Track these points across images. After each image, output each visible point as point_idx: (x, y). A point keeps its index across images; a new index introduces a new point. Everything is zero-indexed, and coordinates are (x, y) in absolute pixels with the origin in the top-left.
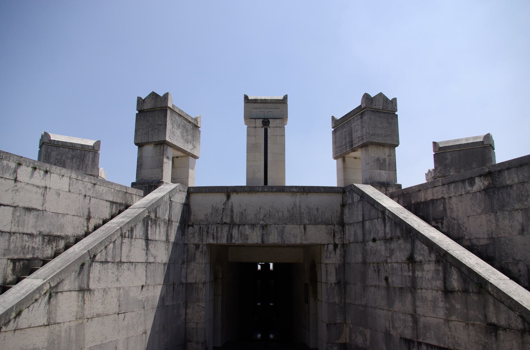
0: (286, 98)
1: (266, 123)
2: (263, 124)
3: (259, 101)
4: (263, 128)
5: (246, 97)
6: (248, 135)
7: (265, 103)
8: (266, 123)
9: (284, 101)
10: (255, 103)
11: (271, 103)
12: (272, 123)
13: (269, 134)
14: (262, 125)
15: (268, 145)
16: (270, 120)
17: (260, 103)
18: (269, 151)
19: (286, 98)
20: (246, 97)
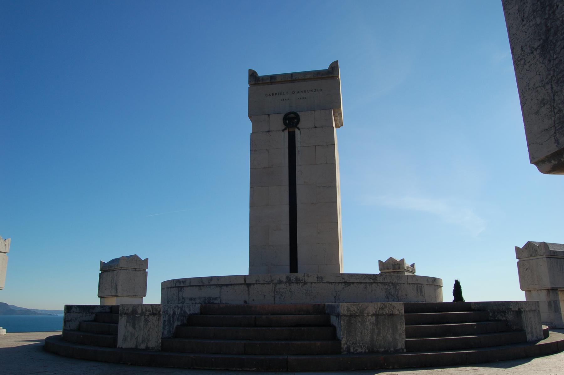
0: (334, 67)
1: (291, 121)
2: (285, 123)
3: (279, 80)
4: (286, 133)
5: (253, 75)
6: (254, 150)
7: (293, 81)
8: (291, 121)
9: (331, 73)
10: (272, 83)
11: (304, 80)
12: (305, 121)
13: (298, 144)
14: (284, 127)
15: (298, 168)
16: (301, 114)
17: (281, 82)
18: (299, 182)
19: (334, 67)
20: (253, 75)
